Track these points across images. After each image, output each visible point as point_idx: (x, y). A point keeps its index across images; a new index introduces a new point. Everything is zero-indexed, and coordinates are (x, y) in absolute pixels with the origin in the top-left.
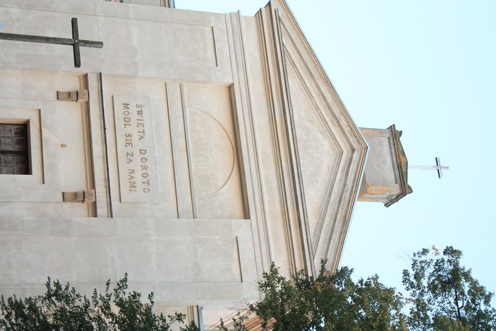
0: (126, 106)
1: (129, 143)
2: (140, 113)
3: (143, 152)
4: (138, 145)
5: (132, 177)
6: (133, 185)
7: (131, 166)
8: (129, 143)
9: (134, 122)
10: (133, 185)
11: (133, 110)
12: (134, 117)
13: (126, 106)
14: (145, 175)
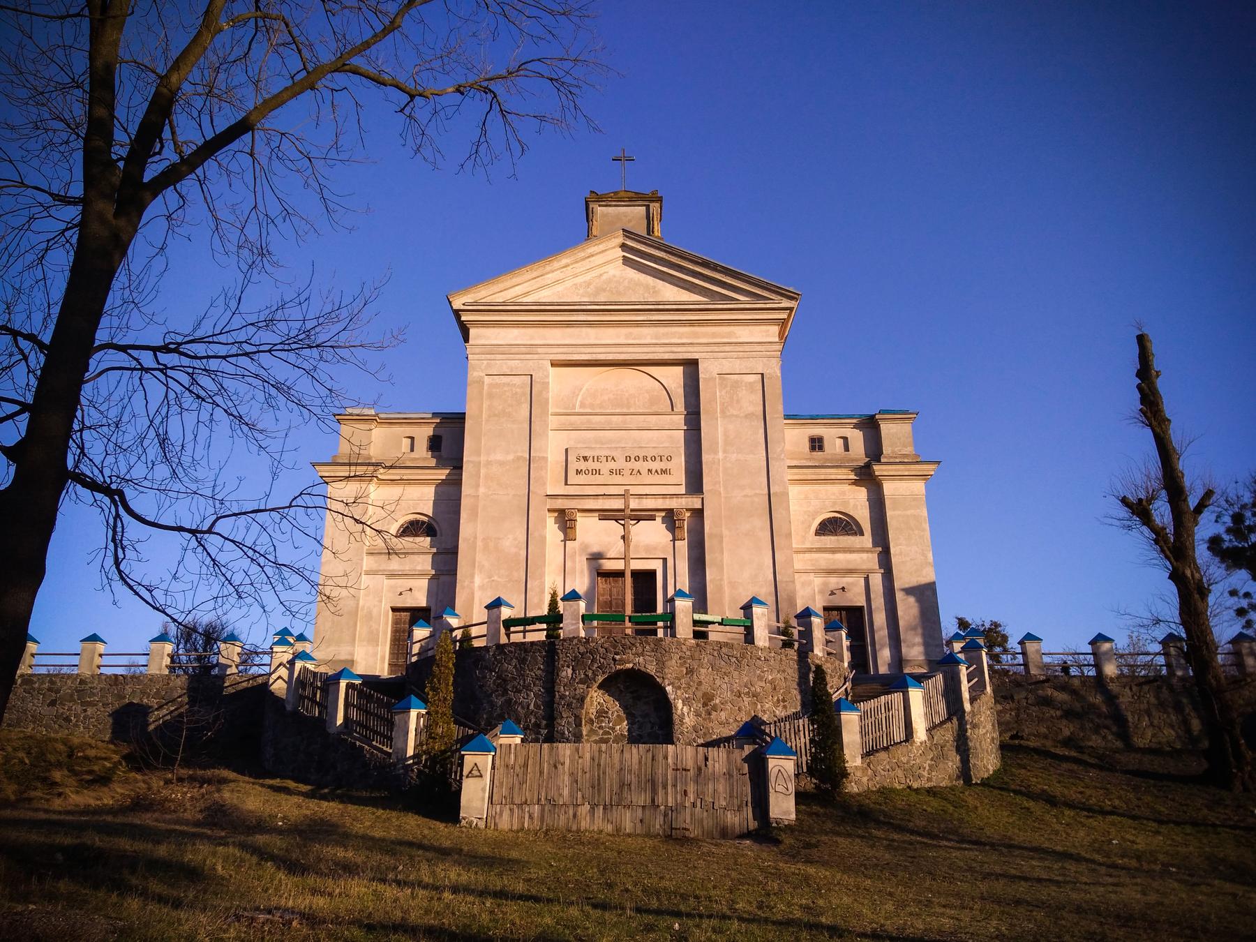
0: (578, 472)
5: (656, 471)
6: (664, 472)
10: (664, 472)
11: (583, 465)
13: (578, 472)
14: (654, 459)
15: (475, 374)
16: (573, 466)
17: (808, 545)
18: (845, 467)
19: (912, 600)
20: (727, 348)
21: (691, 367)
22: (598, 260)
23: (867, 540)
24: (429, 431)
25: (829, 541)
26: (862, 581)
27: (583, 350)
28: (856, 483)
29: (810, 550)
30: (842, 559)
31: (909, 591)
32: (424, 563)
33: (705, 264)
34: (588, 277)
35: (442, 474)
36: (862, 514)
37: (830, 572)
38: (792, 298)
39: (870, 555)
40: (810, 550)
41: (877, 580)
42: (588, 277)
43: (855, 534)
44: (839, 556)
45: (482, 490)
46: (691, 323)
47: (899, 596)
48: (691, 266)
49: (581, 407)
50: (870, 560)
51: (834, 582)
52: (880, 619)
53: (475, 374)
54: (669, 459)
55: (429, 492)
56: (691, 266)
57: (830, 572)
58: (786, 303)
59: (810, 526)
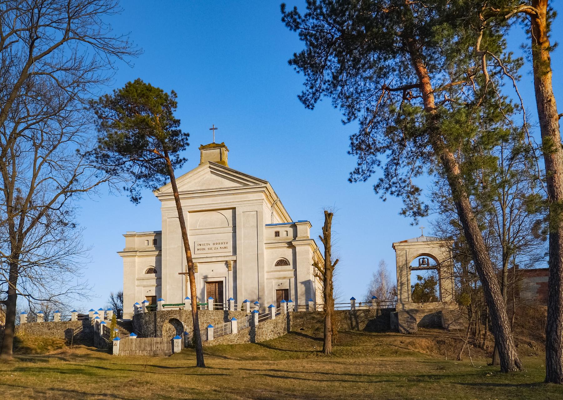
0: (198, 250)
1: (211, 249)
2: (200, 245)
3: (214, 244)
4: (211, 246)
6: (225, 248)
7: (219, 248)
8: (211, 249)
9: (204, 247)
10: (225, 248)
11: (199, 247)
12: (202, 247)
13: (198, 250)
14: (222, 243)
15: (164, 218)
16: (197, 247)
17: (272, 270)
18: (284, 242)
19: (303, 286)
20: (245, 202)
21: (234, 209)
22: (202, 173)
23: (291, 267)
24: (153, 238)
25: (279, 268)
26: (289, 280)
27: (198, 207)
28: (288, 247)
29: (272, 271)
30: (282, 274)
31: (302, 283)
32: (154, 282)
33: (236, 172)
34: (199, 179)
35: (157, 253)
36: (290, 259)
37: (280, 278)
38: (265, 183)
39: (291, 272)
40: (272, 271)
41: (293, 280)
42: (199, 179)
43: (288, 265)
44: (282, 273)
45: (168, 258)
46: (233, 194)
47: (299, 285)
48: (232, 173)
49: (199, 227)
50: (291, 274)
51: (281, 281)
52: (293, 292)
53: (164, 218)
54: (227, 243)
55: (154, 259)
56: (232, 173)
57: (280, 278)
58: (264, 185)
59: (273, 263)
